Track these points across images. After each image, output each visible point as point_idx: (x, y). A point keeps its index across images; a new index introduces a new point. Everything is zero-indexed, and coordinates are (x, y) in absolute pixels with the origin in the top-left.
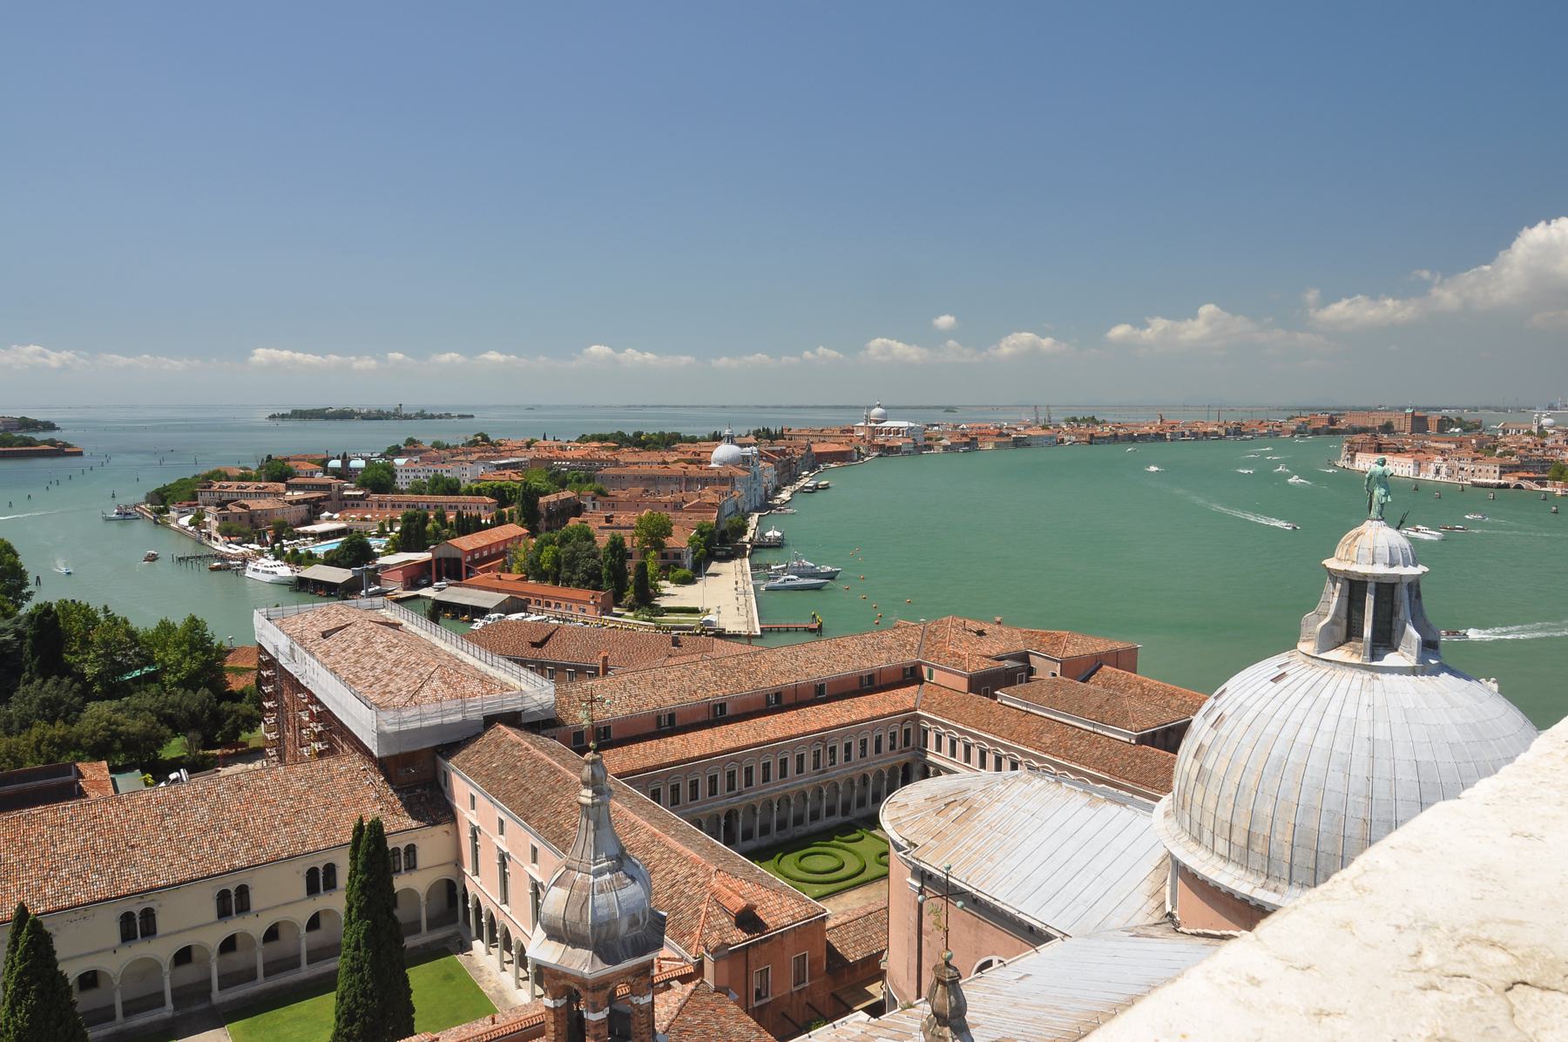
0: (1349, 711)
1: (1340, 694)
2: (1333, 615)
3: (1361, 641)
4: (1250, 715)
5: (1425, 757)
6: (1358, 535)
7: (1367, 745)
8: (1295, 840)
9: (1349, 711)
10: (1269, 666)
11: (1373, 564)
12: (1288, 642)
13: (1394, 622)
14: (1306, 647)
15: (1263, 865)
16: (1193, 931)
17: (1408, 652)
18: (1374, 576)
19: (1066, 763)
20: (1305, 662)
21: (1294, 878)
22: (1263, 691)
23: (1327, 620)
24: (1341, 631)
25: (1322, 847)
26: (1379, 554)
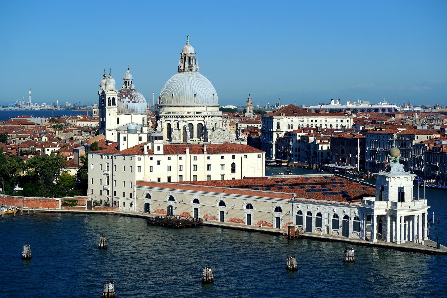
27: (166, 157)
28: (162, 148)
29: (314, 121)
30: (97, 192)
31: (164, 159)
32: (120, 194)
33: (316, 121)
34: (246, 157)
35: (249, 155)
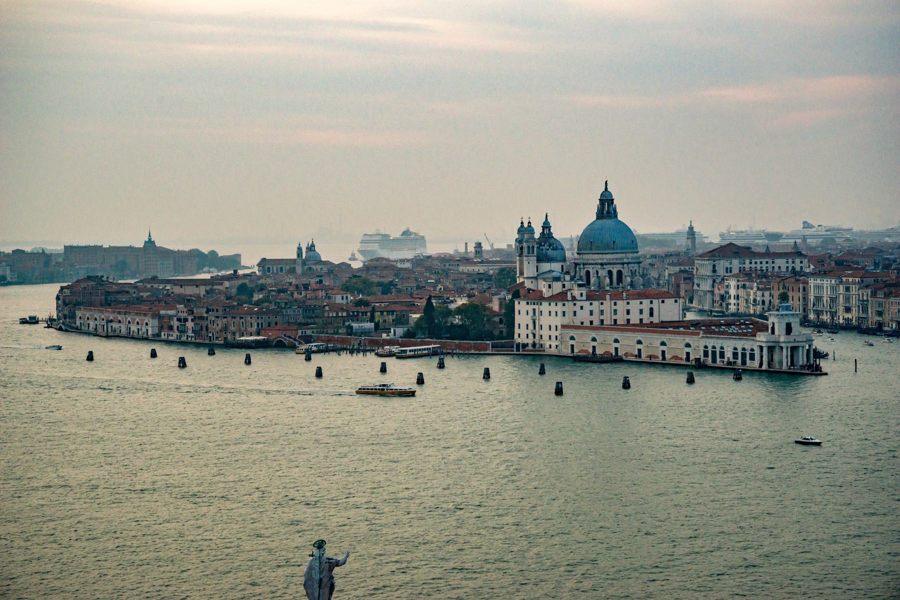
27: (588, 303)
28: (584, 295)
29: (758, 263)
30: (523, 336)
31: (586, 304)
32: (546, 338)
33: (761, 263)
34: (663, 302)
35: (666, 300)
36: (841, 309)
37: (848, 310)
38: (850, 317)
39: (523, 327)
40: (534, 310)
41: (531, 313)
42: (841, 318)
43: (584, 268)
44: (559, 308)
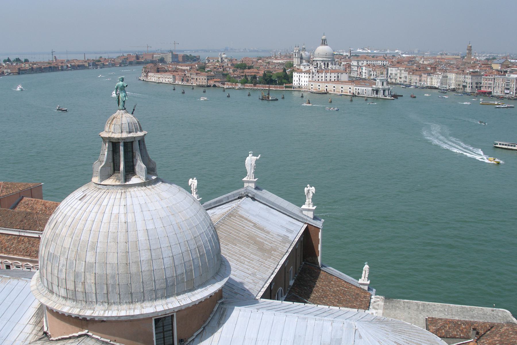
0: (115, 211)
1: (111, 201)
2: (106, 161)
3: (119, 173)
4: (70, 220)
5: (150, 227)
6: (114, 118)
7: (124, 225)
8: (96, 281)
9: (115, 211)
10: (78, 193)
11: (121, 133)
12: (85, 179)
13: (134, 161)
14: (96, 179)
15: (83, 297)
16: (57, 338)
17: (141, 175)
18: (122, 139)
19: (6, 256)
20: (96, 187)
21: (98, 300)
22: (75, 206)
23: (103, 164)
24: (110, 169)
25: (109, 282)
26: (124, 127)
30: (296, 84)
36: (398, 78)
37: (400, 78)
38: (401, 80)
39: (296, 81)
40: (300, 75)
41: (298, 76)
42: (398, 80)
43: (316, 62)
44: (308, 75)
